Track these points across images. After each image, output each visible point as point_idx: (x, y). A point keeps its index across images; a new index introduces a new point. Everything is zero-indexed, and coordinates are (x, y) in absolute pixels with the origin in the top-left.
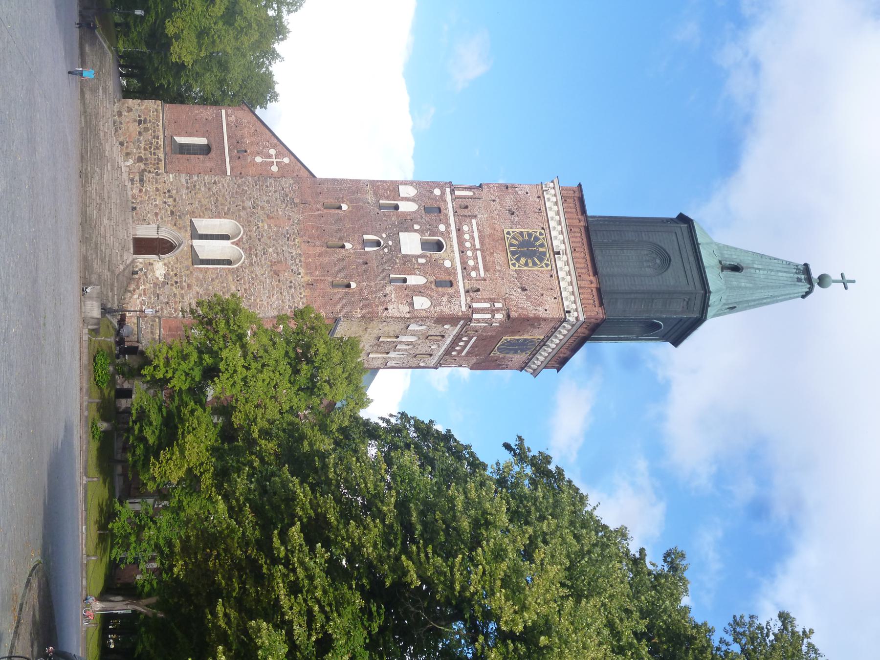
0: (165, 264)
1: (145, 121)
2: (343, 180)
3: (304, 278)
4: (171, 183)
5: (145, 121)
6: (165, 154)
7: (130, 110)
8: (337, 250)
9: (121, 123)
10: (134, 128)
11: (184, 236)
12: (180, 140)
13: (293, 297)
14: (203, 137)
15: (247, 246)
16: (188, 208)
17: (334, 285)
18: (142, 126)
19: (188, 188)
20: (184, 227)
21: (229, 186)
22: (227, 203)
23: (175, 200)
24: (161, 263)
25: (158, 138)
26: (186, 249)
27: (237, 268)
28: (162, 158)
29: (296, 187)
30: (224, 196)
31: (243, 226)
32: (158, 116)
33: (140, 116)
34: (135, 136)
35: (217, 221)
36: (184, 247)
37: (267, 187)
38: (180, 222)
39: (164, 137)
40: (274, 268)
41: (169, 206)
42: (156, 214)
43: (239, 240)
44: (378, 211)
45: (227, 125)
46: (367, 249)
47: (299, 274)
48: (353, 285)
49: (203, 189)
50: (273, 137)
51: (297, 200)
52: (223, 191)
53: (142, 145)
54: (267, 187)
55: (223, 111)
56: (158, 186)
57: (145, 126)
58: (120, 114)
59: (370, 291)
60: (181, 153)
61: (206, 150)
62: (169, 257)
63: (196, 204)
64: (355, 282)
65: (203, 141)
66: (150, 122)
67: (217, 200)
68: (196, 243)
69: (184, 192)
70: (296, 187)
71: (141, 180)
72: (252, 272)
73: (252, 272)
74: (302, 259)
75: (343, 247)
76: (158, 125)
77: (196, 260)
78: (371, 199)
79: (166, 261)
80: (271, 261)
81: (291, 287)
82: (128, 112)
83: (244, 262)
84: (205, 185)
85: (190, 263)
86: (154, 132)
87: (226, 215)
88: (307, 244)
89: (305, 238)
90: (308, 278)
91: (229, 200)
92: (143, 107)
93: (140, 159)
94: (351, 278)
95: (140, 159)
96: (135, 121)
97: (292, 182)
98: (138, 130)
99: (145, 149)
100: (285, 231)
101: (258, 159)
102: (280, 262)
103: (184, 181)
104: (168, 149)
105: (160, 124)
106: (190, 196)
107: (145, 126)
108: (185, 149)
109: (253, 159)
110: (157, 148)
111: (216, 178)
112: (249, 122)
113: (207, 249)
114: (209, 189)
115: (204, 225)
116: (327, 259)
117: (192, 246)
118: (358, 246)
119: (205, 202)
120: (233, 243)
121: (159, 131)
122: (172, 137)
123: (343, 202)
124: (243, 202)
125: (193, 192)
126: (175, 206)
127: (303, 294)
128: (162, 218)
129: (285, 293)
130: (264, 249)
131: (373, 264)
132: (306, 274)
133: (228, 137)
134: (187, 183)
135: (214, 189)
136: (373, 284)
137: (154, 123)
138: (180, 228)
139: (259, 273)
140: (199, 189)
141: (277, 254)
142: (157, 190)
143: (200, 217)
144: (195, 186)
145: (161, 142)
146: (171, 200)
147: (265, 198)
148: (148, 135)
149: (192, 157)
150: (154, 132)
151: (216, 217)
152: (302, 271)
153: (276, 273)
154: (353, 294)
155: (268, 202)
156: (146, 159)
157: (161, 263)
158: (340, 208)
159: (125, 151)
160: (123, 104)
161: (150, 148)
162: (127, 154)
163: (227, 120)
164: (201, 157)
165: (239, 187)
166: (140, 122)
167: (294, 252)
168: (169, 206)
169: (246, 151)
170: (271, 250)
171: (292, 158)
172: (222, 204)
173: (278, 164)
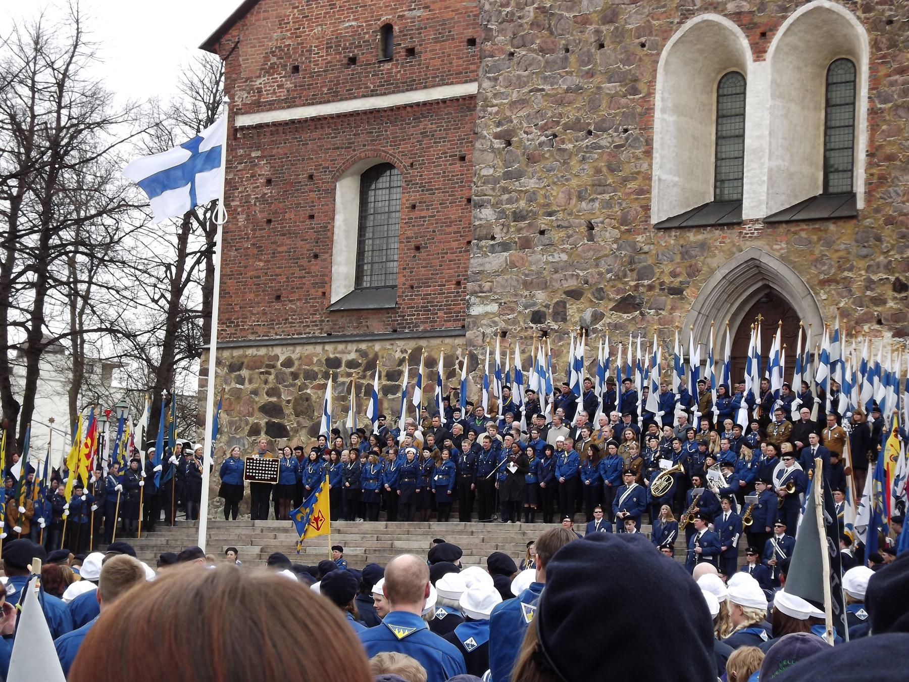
1: (271, 410)
4: (506, 308)
5: (271, 410)
6: (395, 334)
11: (723, 256)
16: (607, 235)
18: (290, 422)
19: (526, 244)
20: (685, 254)
22: (590, 85)
23: (575, 294)
25: (334, 363)
26: (781, 246)
27: (873, 26)
28: (411, 345)
32: (255, 364)
33: (255, 431)
35: (664, 123)
36: (772, 256)
38: (665, 273)
39: (330, 338)
41: (597, 317)
43: (748, 28)
45: (290, 103)
49: (531, 184)
52: (538, 102)
63: (592, 209)
65: (346, 193)
67: (576, 126)
68: (757, 203)
69: (538, 258)
76: (288, 363)
77: (829, 205)
84: (518, 175)
85: (848, 228)
86: (311, 376)
87: (637, 87)
91: (576, 80)
103: (496, 261)
104: (377, 326)
105: (282, 354)
106: (556, 236)
107: (288, 410)
111: (489, 130)
112: (282, 22)
113: (775, 165)
114: (531, 159)
115: (674, 178)
117: (771, 223)
119: (582, 174)
120: (759, 52)
121: (308, 359)
124: (584, 21)
125: (543, 222)
126: (600, 294)
133: (335, 97)
134: (505, 247)
135: (531, 138)
137: (280, 378)
138: (693, 272)
140: (532, 197)
143: (644, 191)
144: (518, 216)
145: (349, 352)
146: (572, 309)
150: (311, 376)
151: (646, 126)
163: (271, 106)
168: (597, 317)
169: (387, 29)
172: (593, 104)
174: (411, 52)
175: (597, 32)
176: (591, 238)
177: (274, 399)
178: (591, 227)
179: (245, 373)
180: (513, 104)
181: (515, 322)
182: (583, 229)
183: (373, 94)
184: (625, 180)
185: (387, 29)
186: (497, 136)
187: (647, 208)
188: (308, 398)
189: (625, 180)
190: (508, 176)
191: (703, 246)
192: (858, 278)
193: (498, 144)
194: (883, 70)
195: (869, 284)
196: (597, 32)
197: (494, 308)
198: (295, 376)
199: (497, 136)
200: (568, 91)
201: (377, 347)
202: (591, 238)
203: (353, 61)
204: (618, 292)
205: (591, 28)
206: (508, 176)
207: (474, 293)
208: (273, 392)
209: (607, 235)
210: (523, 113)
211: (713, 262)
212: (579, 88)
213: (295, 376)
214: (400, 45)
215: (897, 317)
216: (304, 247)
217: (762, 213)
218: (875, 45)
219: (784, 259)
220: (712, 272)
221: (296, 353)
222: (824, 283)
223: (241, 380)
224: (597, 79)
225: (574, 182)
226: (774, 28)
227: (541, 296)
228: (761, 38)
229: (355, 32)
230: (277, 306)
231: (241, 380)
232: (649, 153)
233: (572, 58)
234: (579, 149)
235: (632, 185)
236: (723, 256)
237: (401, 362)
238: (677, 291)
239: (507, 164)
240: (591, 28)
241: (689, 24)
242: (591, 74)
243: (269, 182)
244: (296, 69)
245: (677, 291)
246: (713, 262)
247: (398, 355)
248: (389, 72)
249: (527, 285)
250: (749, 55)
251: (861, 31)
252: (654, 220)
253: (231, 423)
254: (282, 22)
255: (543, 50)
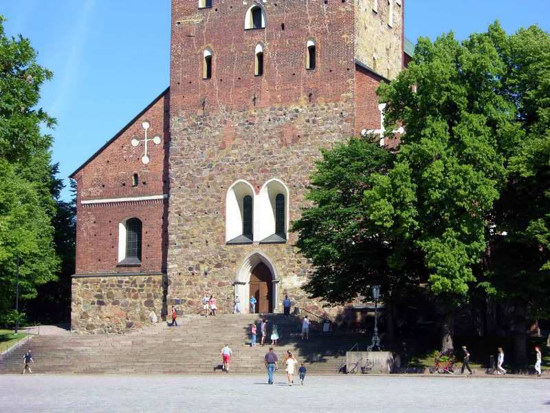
0: (286, 275)
2: (172, 54)
3: (302, 106)
4: (180, 266)
7: (84, 315)
8: (265, 63)
9: (103, 325)
10: (108, 310)
11: (248, 252)
12: (122, 255)
13: (327, 119)
14: (118, 227)
15: (261, 175)
16: (212, 245)
17: (313, 65)
18: (105, 300)
19: (186, 246)
21: (183, 197)
22: (205, 199)
23: (202, 262)
24: (284, 280)
25: (122, 282)
27: (290, 187)
28: (147, 277)
29: (182, 113)
30: (196, 203)
31: (235, 180)
33: (93, 303)
34: (117, 309)
36: (263, 252)
37: (183, 149)
40: (289, 141)
41: (209, 269)
42: (221, 284)
43: (254, 185)
44: (213, 10)
45: (101, 197)
46: (263, 26)
47: (297, 111)
48: (310, 43)
49: (187, 228)
50: (117, 141)
51: (200, 112)
52: (189, 203)
53: (130, 300)
54: (183, 149)
55: (83, 202)
56: (184, 282)
57: (105, 297)
58: (90, 327)
59: (320, 21)
60: (139, 255)
61: (135, 226)
62: (277, 270)
63: (207, 236)
64: (307, 40)
66: (100, 291)
67: (201, 211)
69: (191, 251)
70: (182, 113)
71: (177, 302)
72: (295, 169)
73: (295, 169)
74: (277, 106)
75: (261, 56)
76: (104, 281)
78: (196, 19)
79: (281, 274)
80: (281, 146)
81: (314, 122)
82: (88, 317)
83: (282, 179)
84: (182, 225)
86: (112, 286)
87: (221, 200)
88: (258, 101)
89: (250, 102)
90: (303, 98)
91: (201, 197)
92: (82, 299)
93: (149, 304)
94: (302, 45)
95: (149, 304)
96: (99, 309)
97: (176, 118)
98: (110, 304)
99: (136, 297)
100: (240, 128)
101: (145, 160)
102: (281, 134)
103: (176, 251)
104: (135, 270)
105: (102, 279)
106: (195, 244)
107: (105, 297)
108: (135, 249)
109: (146, 166)
110: (134, 282)
112: (98, 170)
113: (265, 224)
116: (278, 75)
118: (259, 35)
119: (204, 226)
120: (257, 192)
122: (119, 266)
123: (201, 54)
124: (203, 179)
125: (191, 240)
127: (323, 105)
128: (226, 278)
129: (323, 128)
130: (264, 154)
131: (284, 17)
132: (297, 101)
134: (179, 247)
136: (310, 18)
137: (102, 286)
138: (239, 256)
139: (297, 161)
141: (270, 137)
142: (189, 283)
143: (223, 232)
144: (183, 238)
145: (127, 279)
147: (198, 152)
148: (118, 294)
149: (144, 240)
152: (293, 107)
153: (296, 139)
154: (323, 43)
155: (203, 148)
156: (149, 296)
157: (284, 280)
158: (209, 60)
159: (139, 322)
160: (77, 323)
161: (134, 291)
162: (143, 318)
163: (95, 198)
164: (144, 230)
165: (183, 184)
166: (101, 303)
167: (268, 117)
168: (209, 269)
170: (266, 146)
171: (143, 117)
172: (206, 206)
173: (151, 136)
174: (144, 183)
175: (208, 183)
176: (207, 245)
177: (99, 293)
178: (207, 242)
179: (88, 284)
180: (180, 203)
181: (183, 270)
182: (205, 242)
183: (132, 196)
184: (218, 228)
185: (136, 176)
186: (176, 213)
187: (225, 237)
188: (112, 293)
189: (218, 228)
190: (179, 225)
191: (242, 249)
192: (287, 259)
193: (176, 215)
194: (293, 200)
195: (290, 261)
196: (208, 183)
197: (176, 266)
198: (107, 286)
199: (176, 213)
200: (199, 200)
201: (136, 277)
202: (207, 245)
203: (124, 185)
204: (216, 261)
205: (206, 181)
206: (179, 225)
207: (170, 261)
208: (100, 291)
209: (212, 245)
210: (185, 206)
211: (245, 254)
212: (202, 200)
213: (107, 286)
214: (141, 181)
215: (298, 271)
216: (109, 244)
217: (260, 239)
218: (291, 192)
219: (266, 253)
220: (245, 256)
221: (107, 279)
222: (278, 261)
223: (88, 287)
224: (209, 197)
225: (201, 228)
226: (261, 185)
227: (191, 263)
228: (258, 188)
229: (125, 176)
230: (99, 263)
231: (88, 287)
232: (225, 220)
233: (200, 191)
234: (202, 218)
235: (220, 230)
236: (248, 252)
237: (144, 281)
238: (234, 262)
239: (179, 221)
240: (206, 181)
241: (236, 182)
242: (205, 195)
243: (95, 222)
244: (103, 186)
245: (234, 262)
246: (245, 254)
247: (143, 280)
248: (137, 189)
249: (187, 259)
250: (254, 193)
251: (286, 188)
252: (228, 239)
253: (84, 301)
254: (98, 170)
255: (189, 187)
